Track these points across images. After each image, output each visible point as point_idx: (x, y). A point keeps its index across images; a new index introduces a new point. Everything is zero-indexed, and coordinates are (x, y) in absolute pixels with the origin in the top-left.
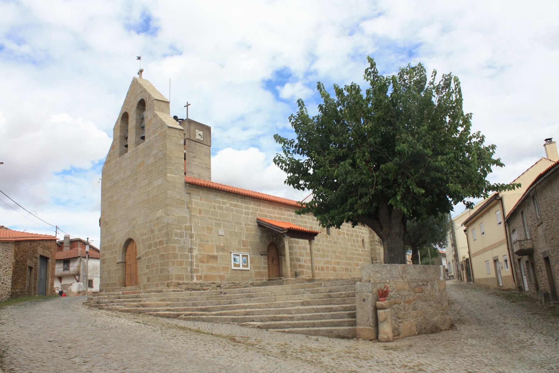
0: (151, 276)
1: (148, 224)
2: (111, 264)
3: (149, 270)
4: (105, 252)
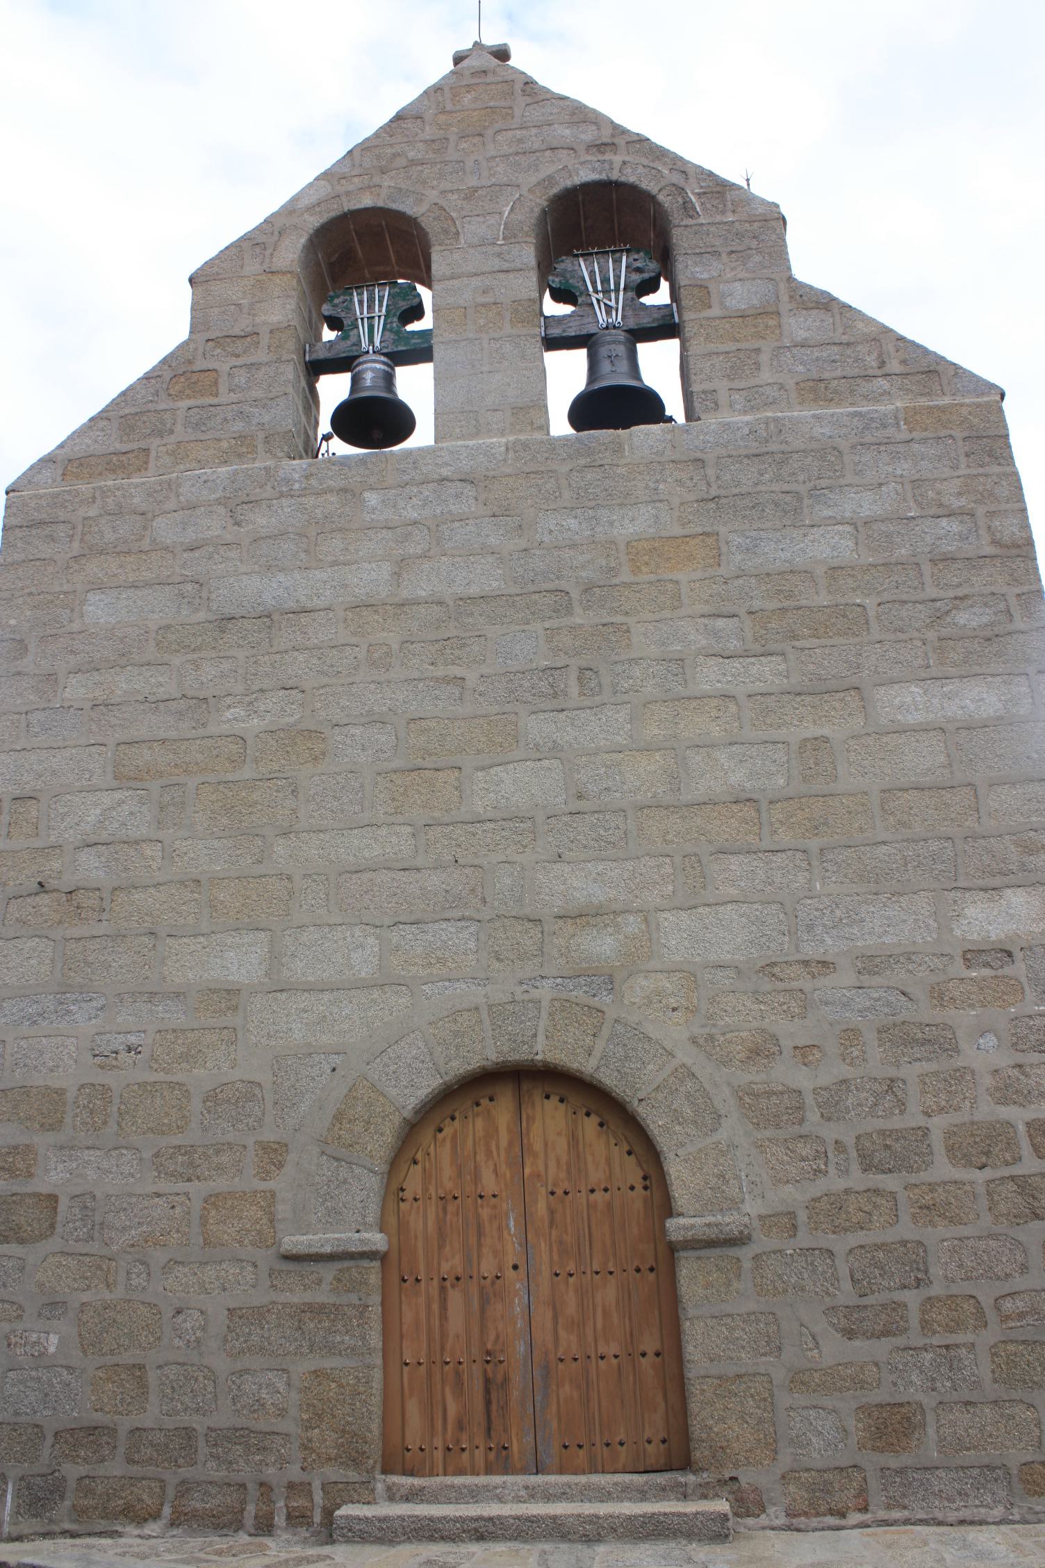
0: (928, 1401)
1: (845, 977)
2: (159, 1257)
3: (900, 1341)
4: (41, 1141)
